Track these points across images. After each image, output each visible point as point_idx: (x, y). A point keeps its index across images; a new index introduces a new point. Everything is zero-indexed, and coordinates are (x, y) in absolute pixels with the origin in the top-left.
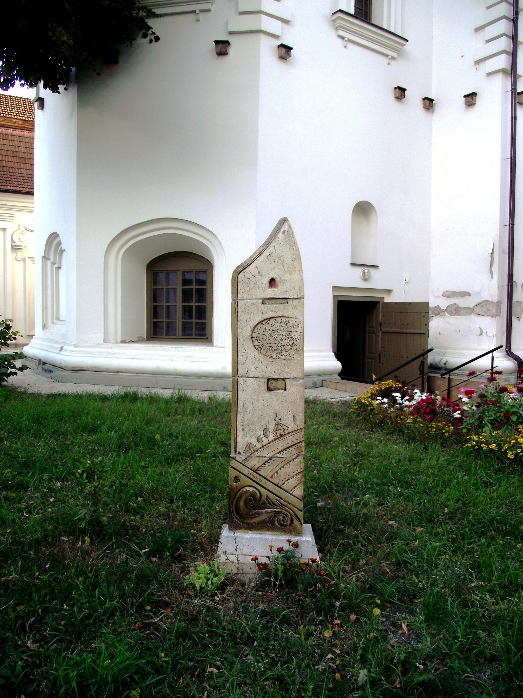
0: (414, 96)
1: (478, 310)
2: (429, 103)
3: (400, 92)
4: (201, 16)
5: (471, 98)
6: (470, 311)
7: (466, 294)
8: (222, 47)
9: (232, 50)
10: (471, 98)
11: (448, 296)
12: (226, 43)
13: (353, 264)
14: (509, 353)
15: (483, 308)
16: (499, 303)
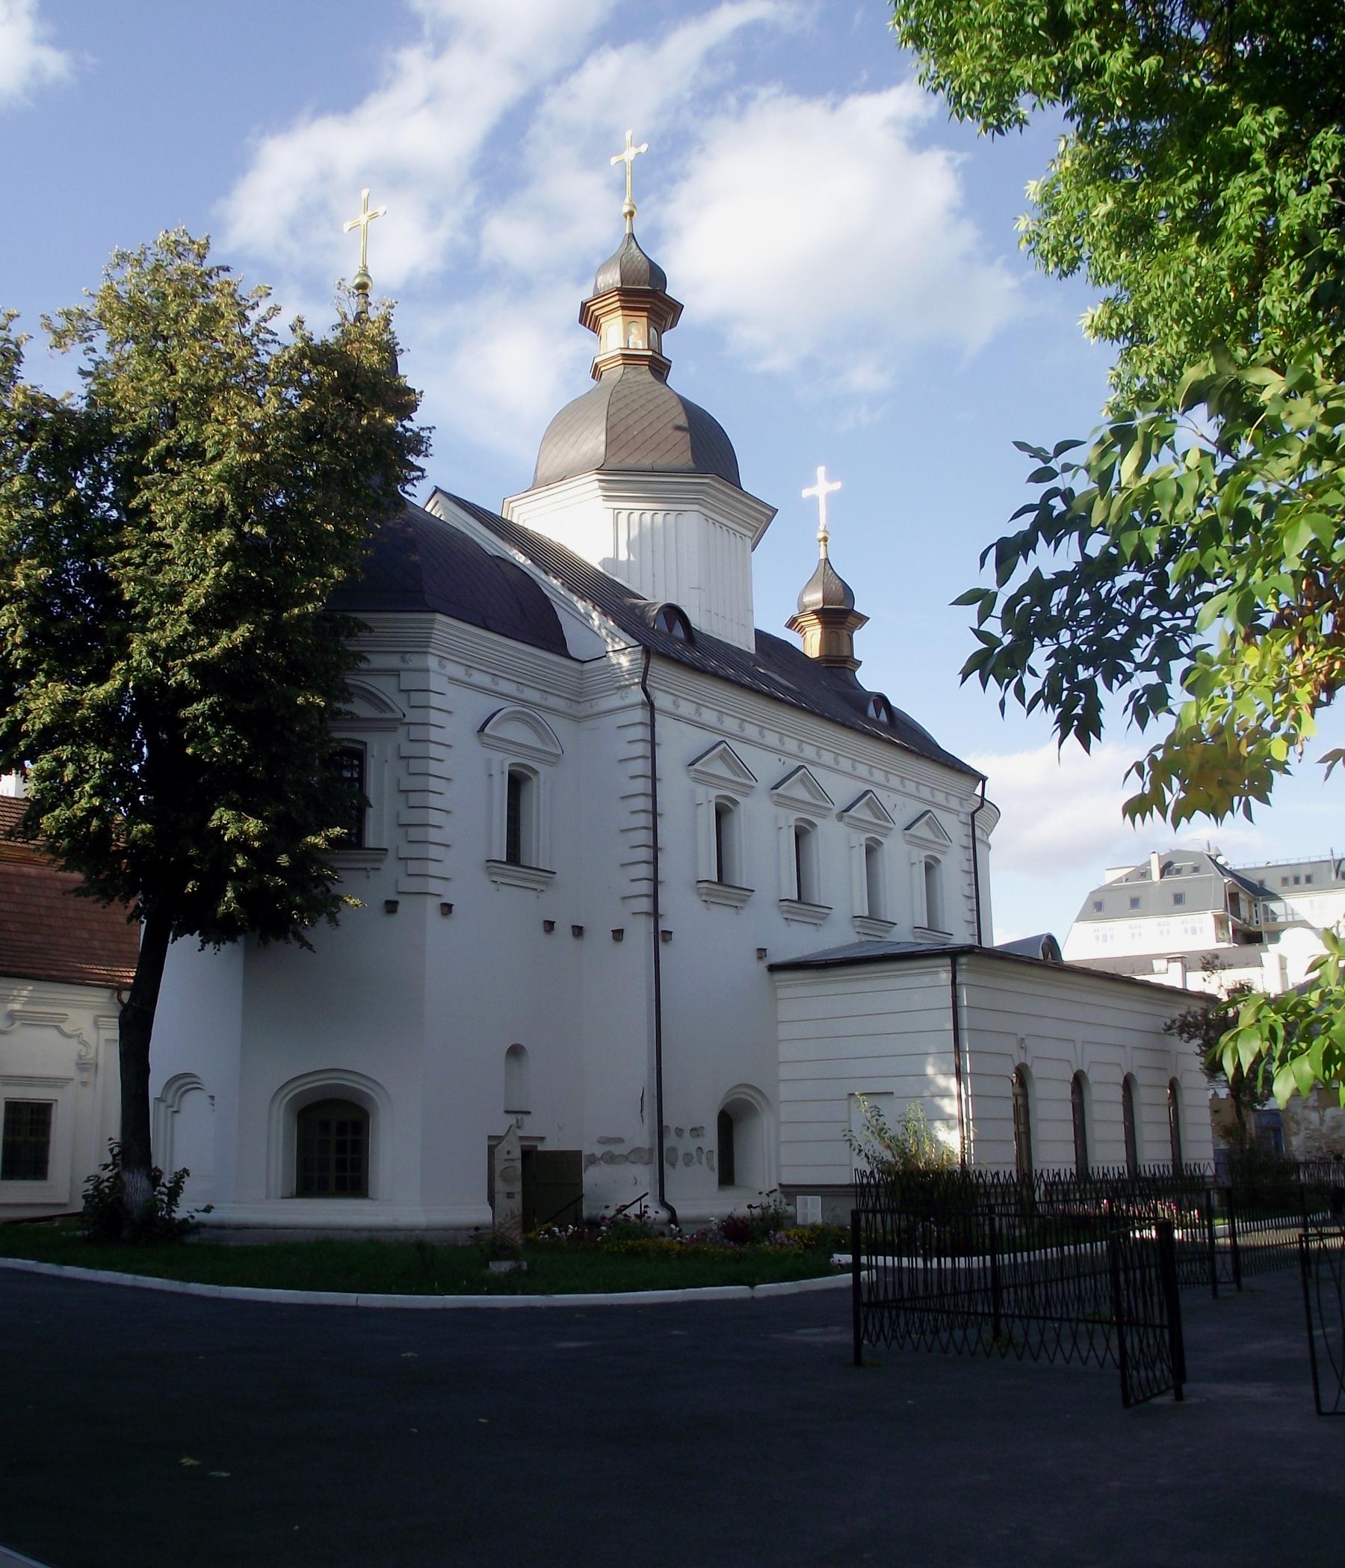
0: (563, 928)
1: (632, 1158)
2: (578, 931)
3: (549, 926)
4: (372, 874)
5: (618, 934)
6: (625, 1158)
7: (620, 1140)
8: (391, 907)
9: (400, 908)
10: (618, 934)
11: (603, 1143)
12: (396, 903)
13: (507, 1112)
14: (663, 1203)
15: (635, 1155)
16: (651, 1149)
